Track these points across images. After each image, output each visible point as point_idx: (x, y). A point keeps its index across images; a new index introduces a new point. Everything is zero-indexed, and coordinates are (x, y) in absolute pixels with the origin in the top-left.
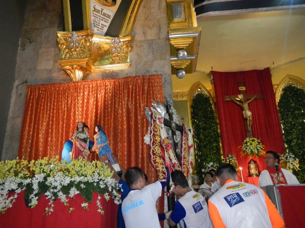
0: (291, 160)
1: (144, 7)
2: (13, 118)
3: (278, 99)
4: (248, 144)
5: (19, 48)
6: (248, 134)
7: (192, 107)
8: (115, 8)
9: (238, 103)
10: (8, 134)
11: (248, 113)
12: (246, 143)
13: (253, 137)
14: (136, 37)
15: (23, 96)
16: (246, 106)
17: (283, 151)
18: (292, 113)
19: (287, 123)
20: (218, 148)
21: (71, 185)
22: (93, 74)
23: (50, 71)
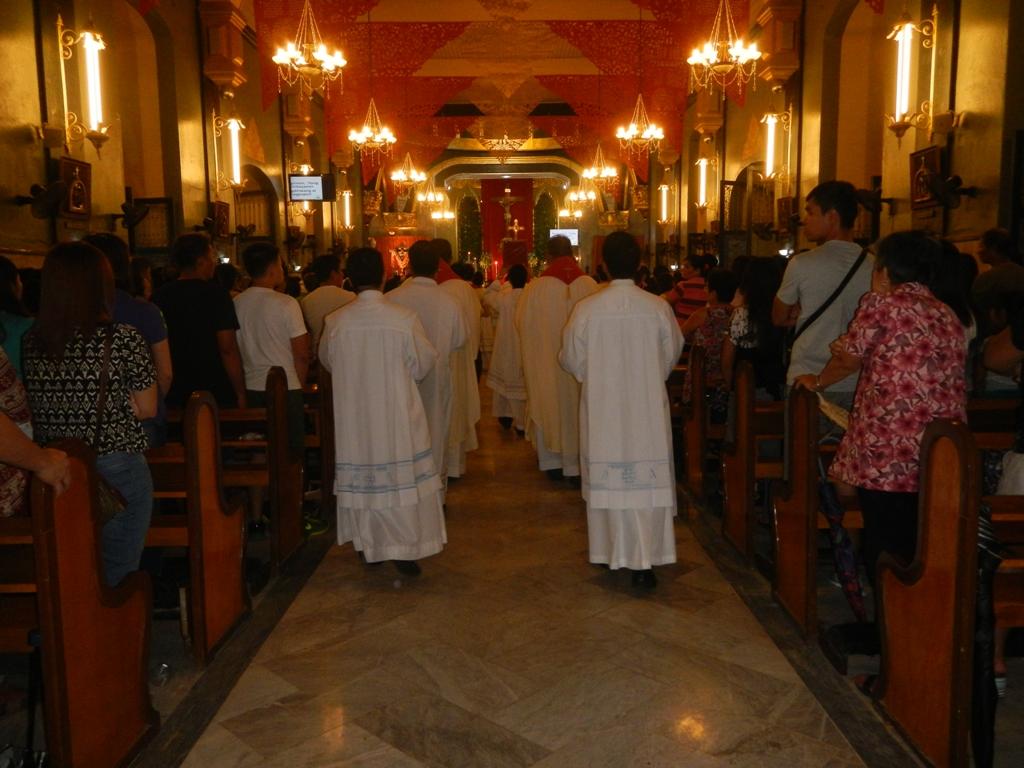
16: (507, 209)
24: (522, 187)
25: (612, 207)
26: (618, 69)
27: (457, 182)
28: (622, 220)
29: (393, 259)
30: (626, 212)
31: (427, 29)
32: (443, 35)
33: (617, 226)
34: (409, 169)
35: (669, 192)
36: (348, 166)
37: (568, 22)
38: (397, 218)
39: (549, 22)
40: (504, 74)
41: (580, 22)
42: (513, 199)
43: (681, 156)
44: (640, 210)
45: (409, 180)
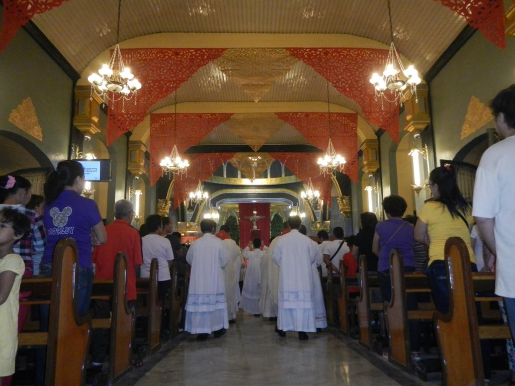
8: (193, 212)
16: (255, 223)
24: (263, 208)
25: (319, 219)
26: (343, 82)
27: (225, 207)
28: (326, 227)
30: (329, 221)
31: (194, 53)
32: (206, 57)
34: (175, 157)
35: (373, 192)
36: (140, 173)
37: (303, 49)
38: (186, 225)
39: (288, 49)
40: (253, 85)
41: (311, 49)
43: (380, 166)
44: (345, 212)
45: (175, 166)
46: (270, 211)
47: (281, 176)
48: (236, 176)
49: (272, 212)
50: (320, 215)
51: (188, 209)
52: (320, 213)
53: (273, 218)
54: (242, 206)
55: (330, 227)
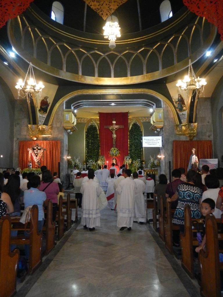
0: (128, 159)
1: (57, 114)
2: (15, 150)
3: (130, 129)
4: (112, 151)
5: (14, 126)
6: (113, 145)
7: (86, 132)
8: (46, 114)
9: (111, 130)
10: (14, 155)
11: (115, 136)
12: (112, 150)
13: (116, 148)
14: (54, 125)
15: (17, 144)
16: (114, 132)
17: (127, 154)
18: (133, 137)
19: (131, 141)
20: (98, 153)
21: (38, 173)
22: (40, 138)
23: (25, 135)
24: (122, 118)
25: (185, 121)
27: (88, 119)
28: (192, 130)
29: (30, 155)
30: (196, 124)
33: (189, 133)
42: (117, 127)
46: (129, 122)
47: (143, 74)
48: (94, 76)
49: (130, 123)
50: (186, 116)
51: (40, 111)
52: (186, 115)
53: (132, 128)
54: (101, 115)
55: (197, 129)
